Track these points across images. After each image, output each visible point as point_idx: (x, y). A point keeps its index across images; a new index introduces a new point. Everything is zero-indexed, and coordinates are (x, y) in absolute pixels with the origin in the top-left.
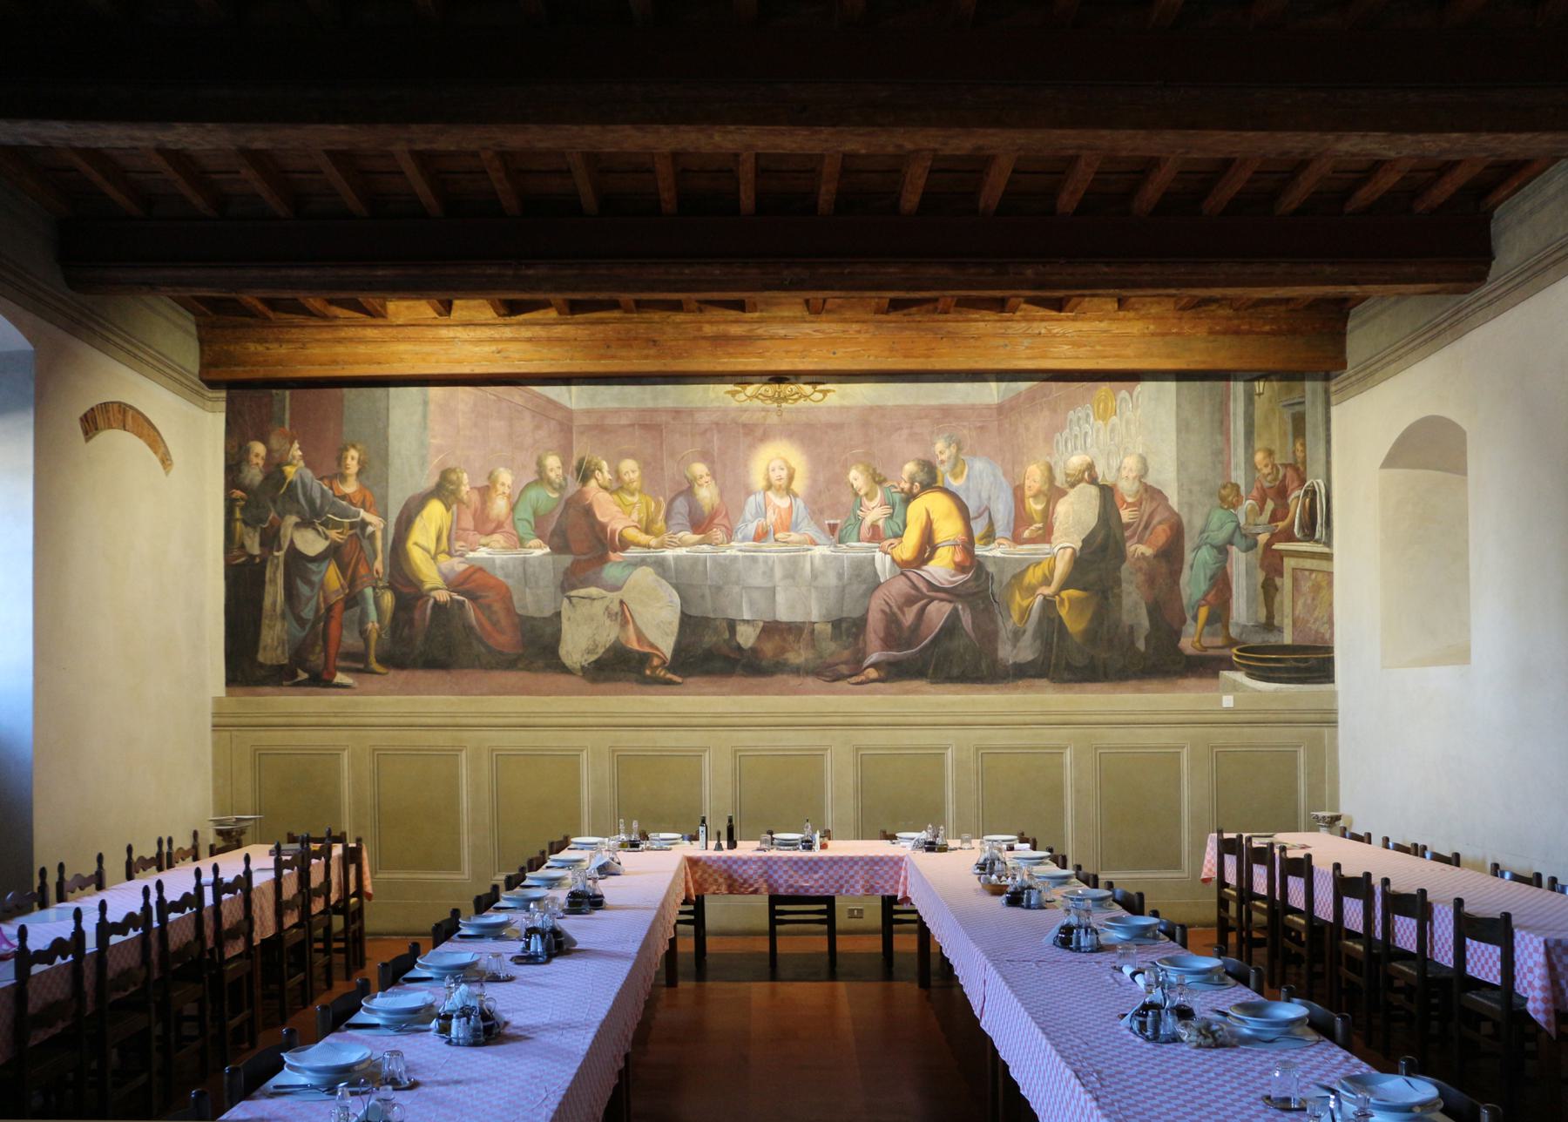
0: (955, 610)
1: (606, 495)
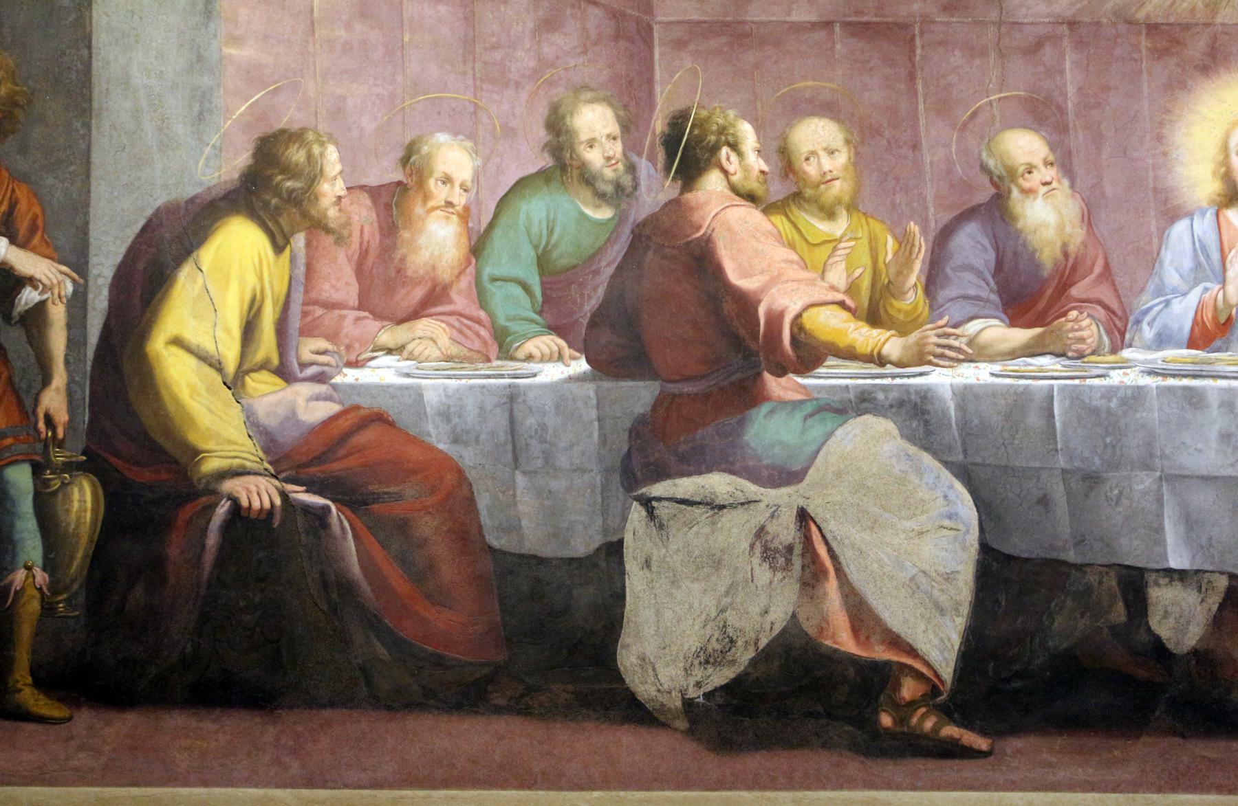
1: (753, 215)
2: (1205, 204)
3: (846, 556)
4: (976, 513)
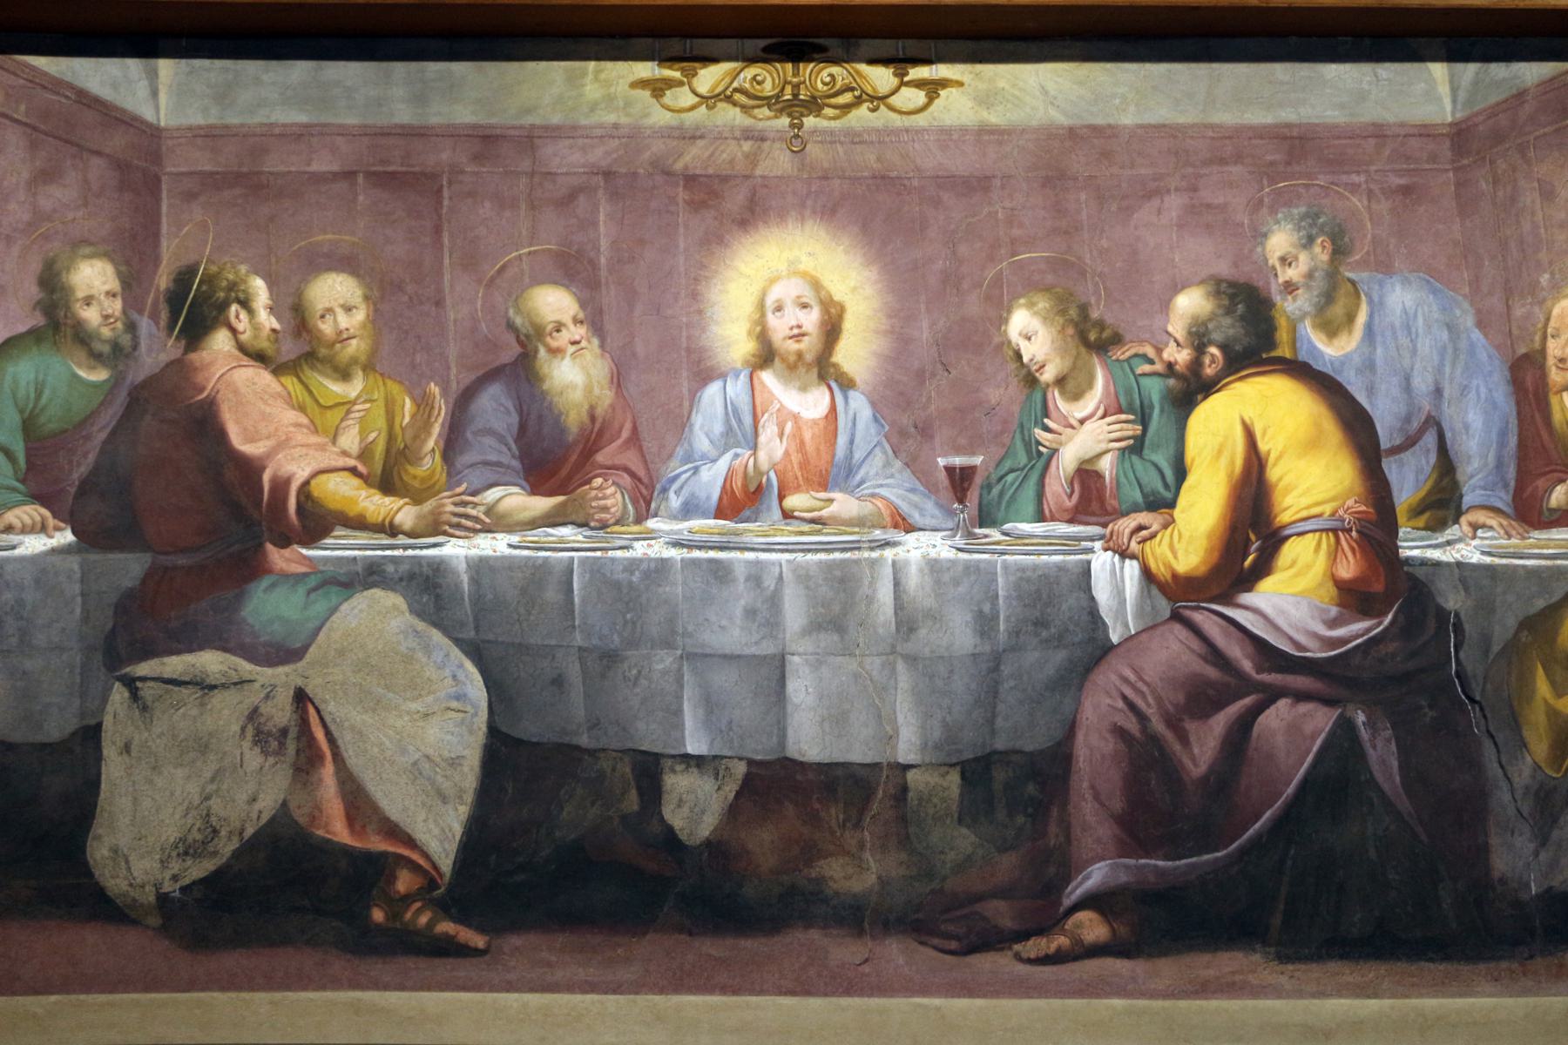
0: (1345, 727)
1: (264, 377)
2: (739, 365)
3: (345, 739)
4: (486, 694)
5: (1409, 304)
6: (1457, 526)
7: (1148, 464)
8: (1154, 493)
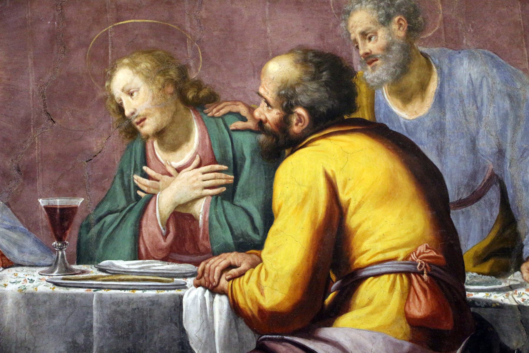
5: (474, 76)
6: (518, 273)
7: (239, 210)
8: (244, 235)
